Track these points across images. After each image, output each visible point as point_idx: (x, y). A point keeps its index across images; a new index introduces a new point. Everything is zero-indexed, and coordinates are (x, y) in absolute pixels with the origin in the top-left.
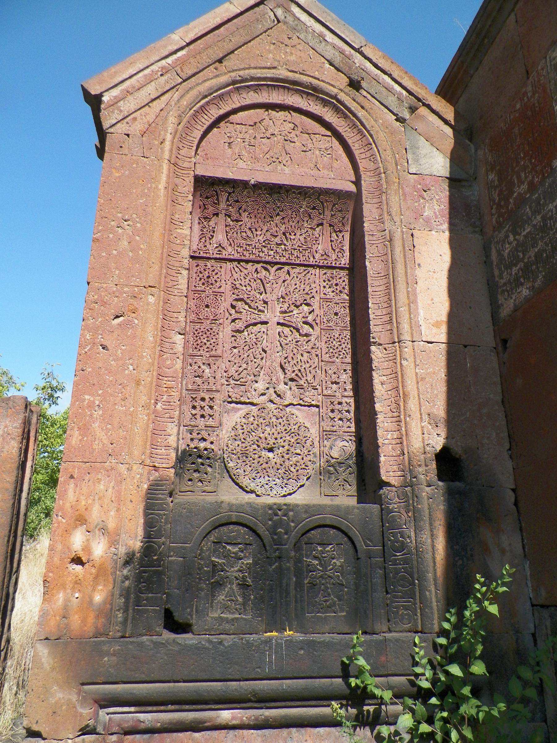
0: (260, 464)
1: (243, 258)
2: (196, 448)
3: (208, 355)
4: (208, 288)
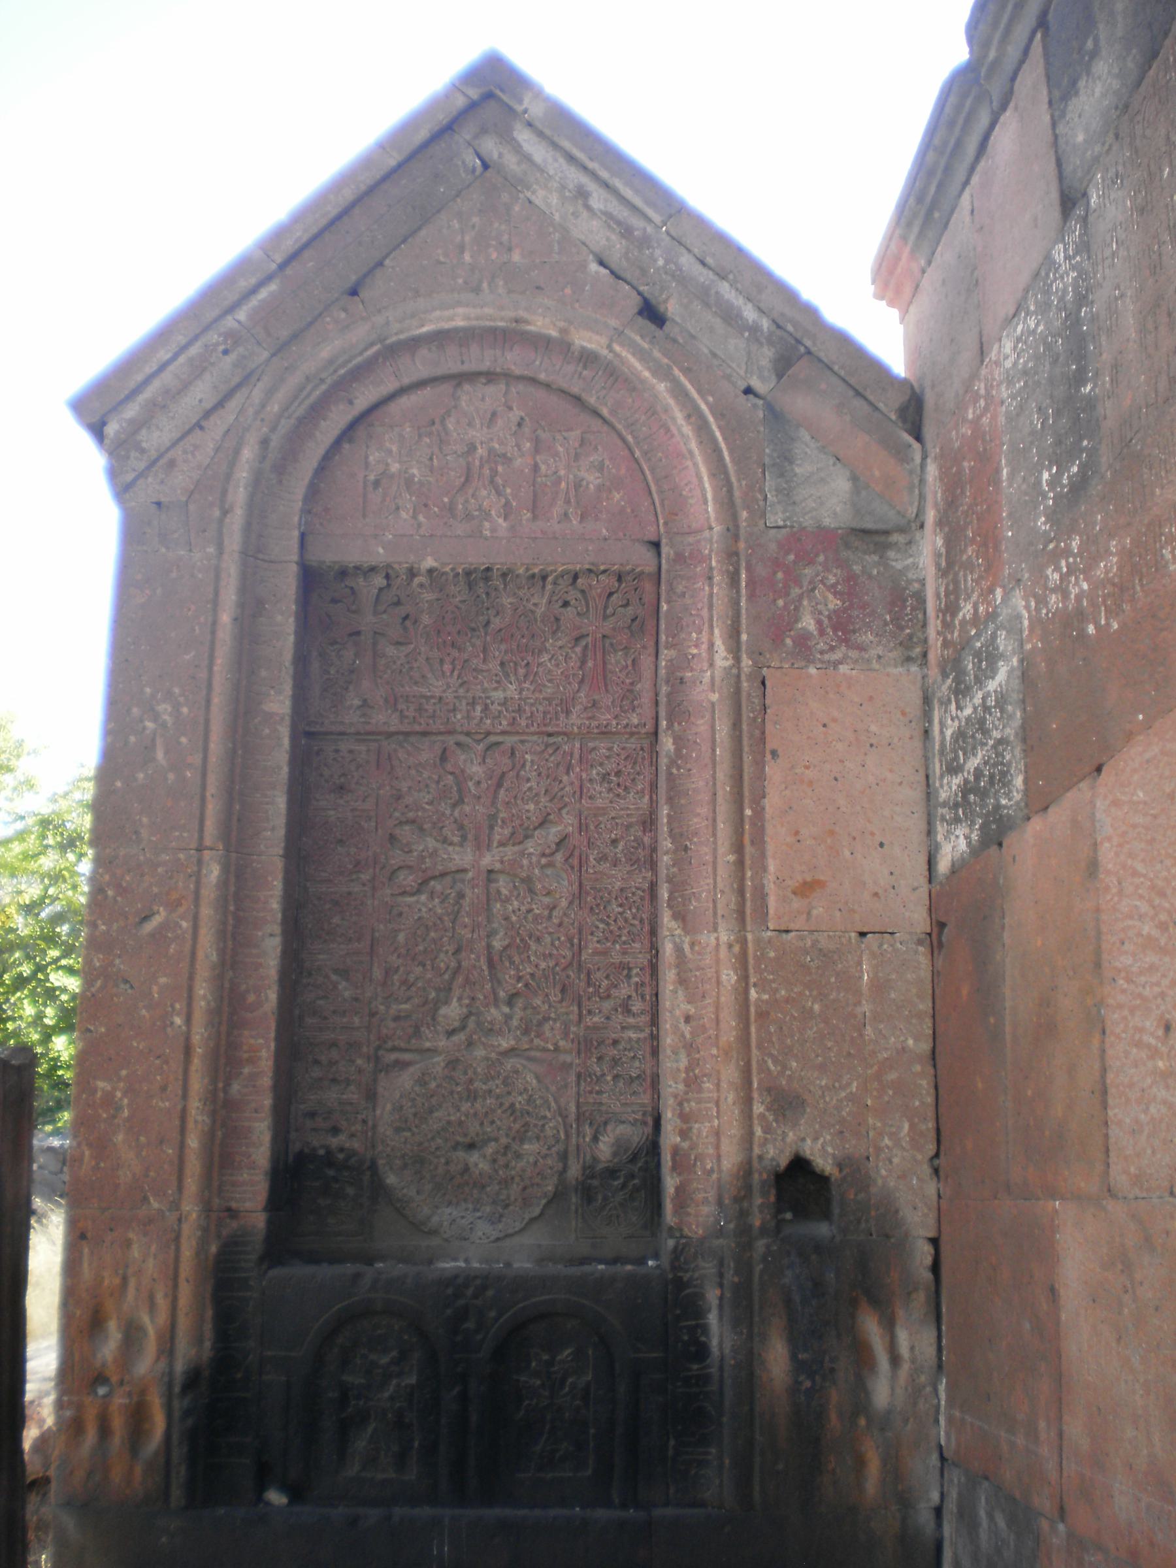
1: (417, 728)
2: (322, 1147)
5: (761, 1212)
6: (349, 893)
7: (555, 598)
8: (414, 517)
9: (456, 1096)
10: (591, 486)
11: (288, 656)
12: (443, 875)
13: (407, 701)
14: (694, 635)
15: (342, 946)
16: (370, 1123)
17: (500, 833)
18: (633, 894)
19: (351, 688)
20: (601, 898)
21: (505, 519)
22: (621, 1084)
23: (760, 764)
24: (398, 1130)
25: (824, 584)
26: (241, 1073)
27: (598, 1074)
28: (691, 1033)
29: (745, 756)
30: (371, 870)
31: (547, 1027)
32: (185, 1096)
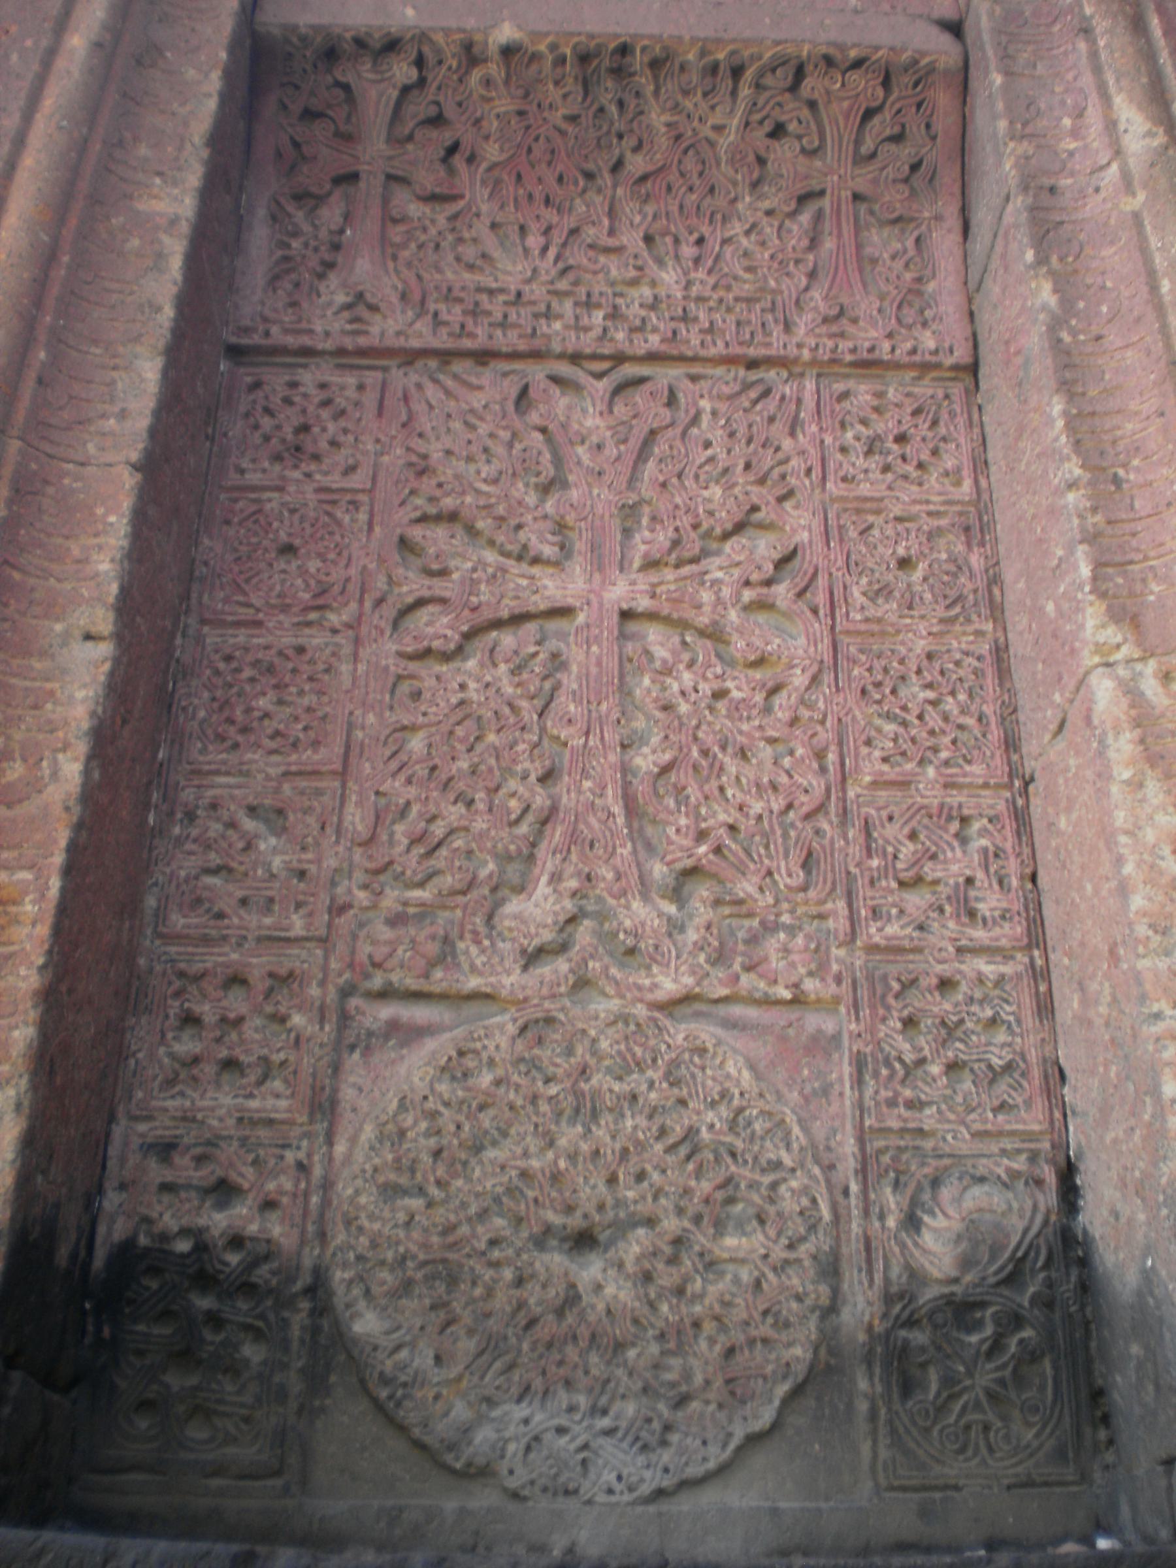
1: (467, 344)
2: (185, 1232)
4: (297, 474)
6: (301, 650)
7: (757, 117)
9: (544, 1107)
12: (518, 619)
13: (446, 299)
14: (1067, 122)
15: (275, 758)
16: (317, 1172)
17: (649, 539)
18: (958, 663)
20: (886, 670)
22: (967, 1085)
24: (390, 1192)
27: (909, 1058)
30: (354, 606)
31: (772, 945)
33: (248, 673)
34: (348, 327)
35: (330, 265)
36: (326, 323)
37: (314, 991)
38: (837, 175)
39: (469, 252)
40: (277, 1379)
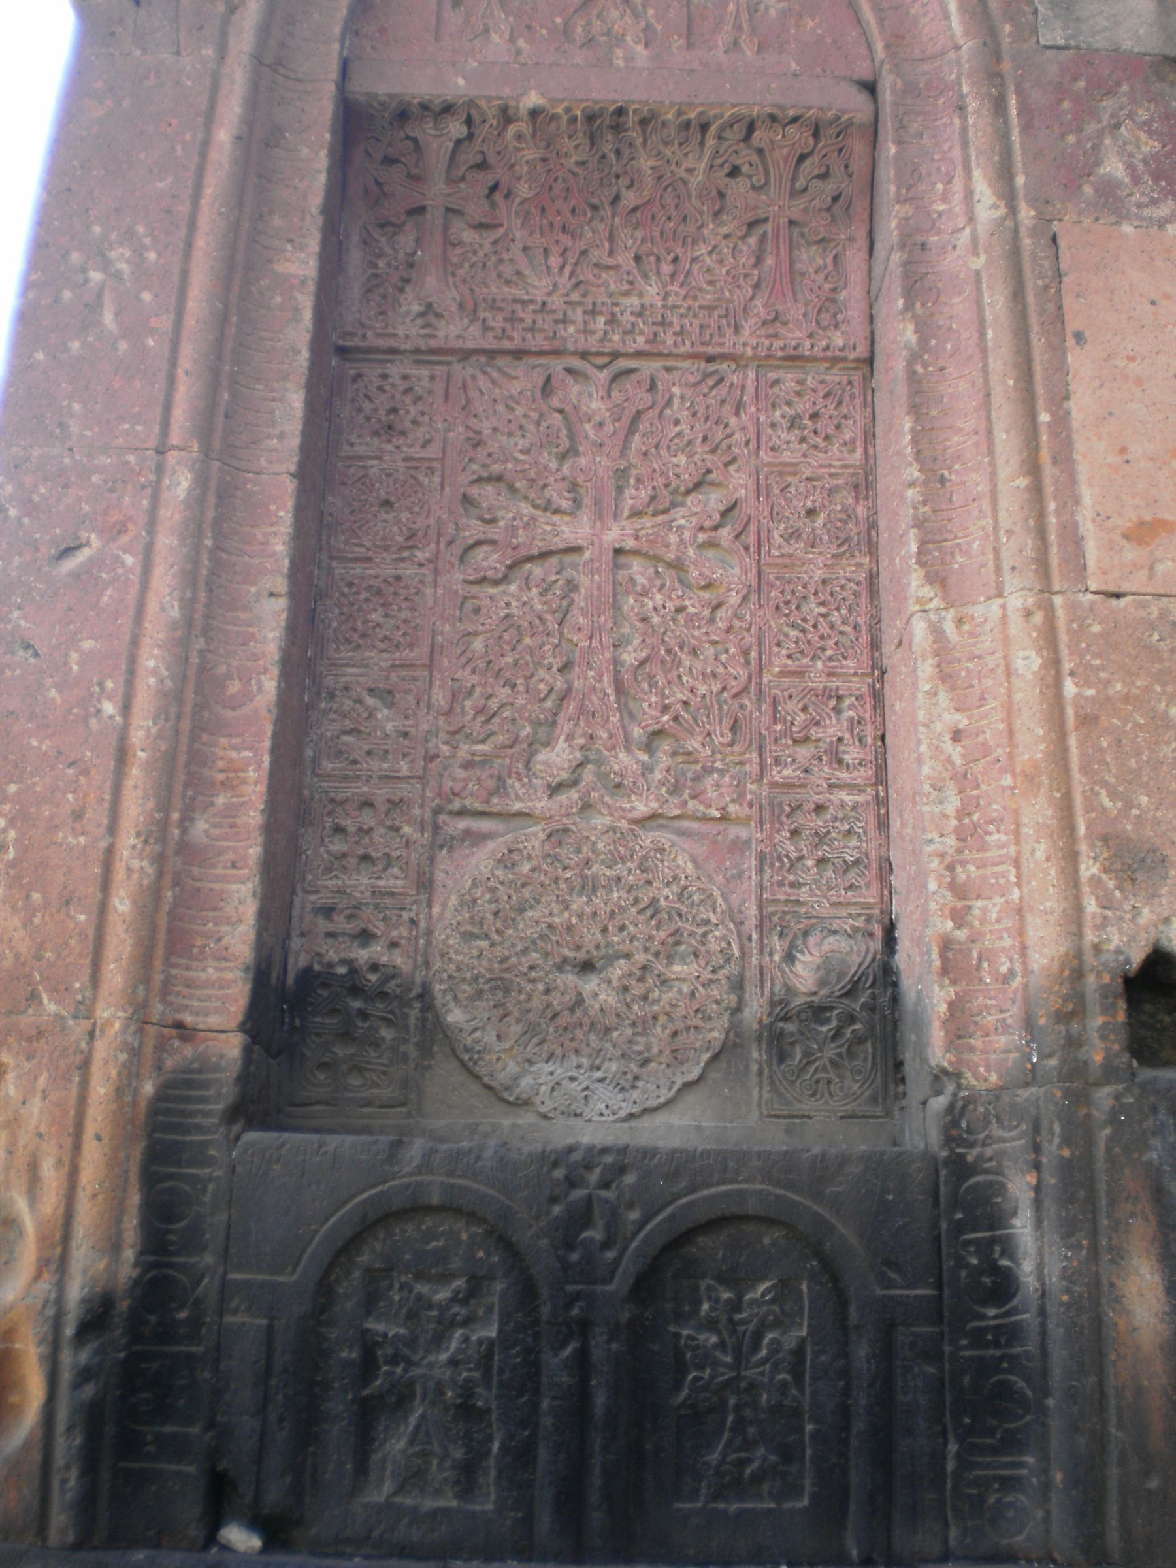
0: (549, 1013)
1: (507, 344)
2: (343, 962)
3: (386, 660)
4: (389, 447)
5: (1103, 1038)
6: (398, 578)
7: (719, 161)
8: (512, 40)
9: (563, 885)
10: (772, 12)
11: (316, 201)
12: (545, 555)
13: (492, 308)
14: (940, 186)
15: (384, 655)
17: (635, 495)
18: (842, 587)
19: (408, 289)
20: (793, 592)
21: (646, 46)
22: (830, 873)
23: (1058, 350)
24: (468, 937)
25: (1134, 121)
26: (212, 804)
27: (793, 855)
28: (963, 756)
29: (1034, 338)
30: (433, 546)
31: (709, 781)
32: (113, 829)
33: (363, 595)
34: (422, 332)
35: (407, 281)
36: (407, 330)
37: (417, 811)
38: (777, 206)
39: (507, 270)
40: (402, 1048)
